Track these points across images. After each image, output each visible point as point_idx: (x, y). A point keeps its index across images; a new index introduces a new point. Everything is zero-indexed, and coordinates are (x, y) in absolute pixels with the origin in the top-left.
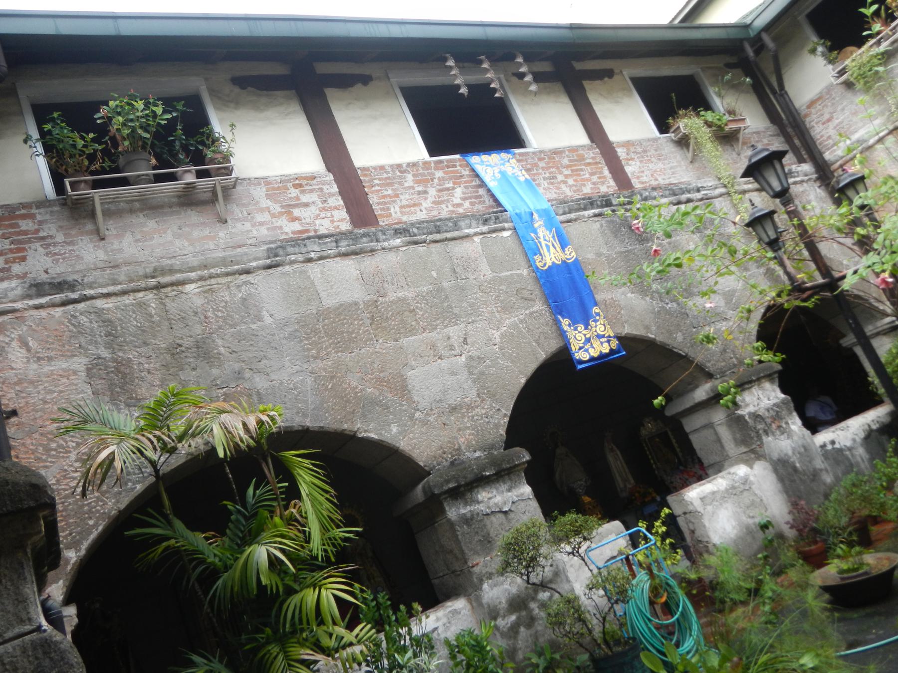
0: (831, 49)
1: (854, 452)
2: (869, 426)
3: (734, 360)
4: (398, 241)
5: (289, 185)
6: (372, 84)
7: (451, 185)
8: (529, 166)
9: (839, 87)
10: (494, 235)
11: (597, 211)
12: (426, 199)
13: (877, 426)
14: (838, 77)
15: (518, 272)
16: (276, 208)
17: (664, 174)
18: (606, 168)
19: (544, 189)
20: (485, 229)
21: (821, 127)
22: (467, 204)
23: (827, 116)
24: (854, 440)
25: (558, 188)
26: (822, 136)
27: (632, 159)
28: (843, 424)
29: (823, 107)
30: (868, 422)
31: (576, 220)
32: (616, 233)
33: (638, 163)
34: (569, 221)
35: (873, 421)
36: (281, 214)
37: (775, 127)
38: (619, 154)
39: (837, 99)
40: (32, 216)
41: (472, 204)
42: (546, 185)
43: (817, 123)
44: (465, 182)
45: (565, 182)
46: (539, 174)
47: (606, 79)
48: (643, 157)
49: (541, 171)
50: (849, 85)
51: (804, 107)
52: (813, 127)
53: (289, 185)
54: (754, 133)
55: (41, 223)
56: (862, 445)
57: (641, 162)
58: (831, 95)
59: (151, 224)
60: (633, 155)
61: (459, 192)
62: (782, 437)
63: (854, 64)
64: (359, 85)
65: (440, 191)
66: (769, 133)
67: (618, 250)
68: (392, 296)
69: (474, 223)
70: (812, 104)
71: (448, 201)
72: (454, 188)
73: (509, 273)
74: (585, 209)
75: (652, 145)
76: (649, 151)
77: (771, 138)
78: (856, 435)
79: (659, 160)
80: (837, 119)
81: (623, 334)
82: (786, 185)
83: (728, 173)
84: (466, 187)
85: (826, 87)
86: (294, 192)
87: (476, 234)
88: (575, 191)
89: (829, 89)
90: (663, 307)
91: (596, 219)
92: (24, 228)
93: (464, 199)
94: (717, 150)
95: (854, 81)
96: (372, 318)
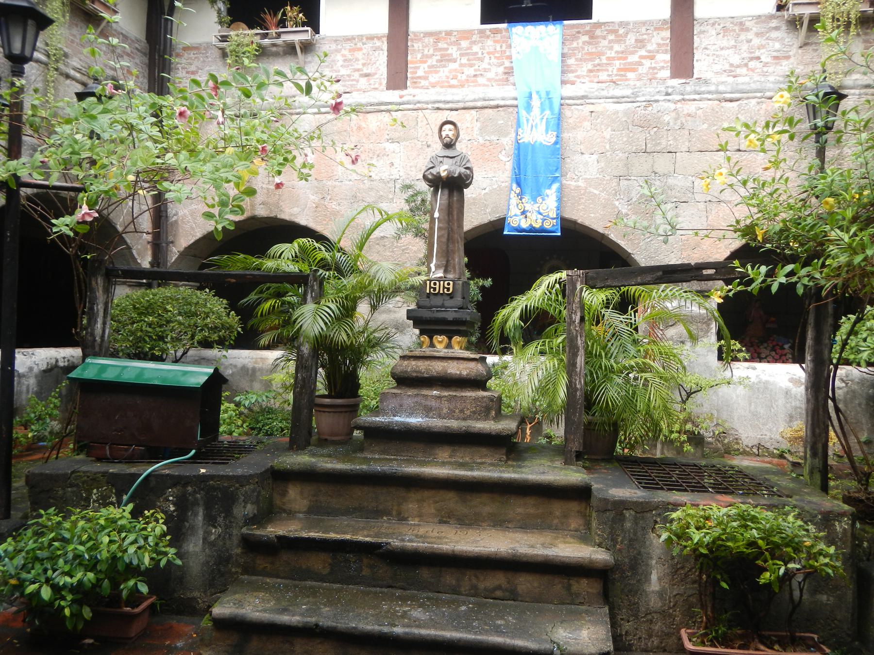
0: (230, 12)
1: (24, 380)
2: (57, 361)
9: (217, 50)
13: (66, 364)
14: (221, 41)
21: (184, 74)
23: (193, 68)
24: (31, 369)
26: (180, 82)
28: (30, 350)
29: (196, 58)
30: (58, 357)
35: (64, 358)
37: (147, 45)
39: (210, 59)
43: (182, 68)
50: (224, 54)
51: (181, 47)
52: (178, 69)
54: (122, 34)
56: (36, 376)
58: (207, 52)
63: (236, 38)
66: (137, 45)
70: (186, 49)
77: (135, 51)
78: (38, 365)
80: (200, 77)
82: (27, 53)
83: (59, 46)
85: (207, 43)
89: (208, 46)
94: (64, 16)
95: (229, 53)
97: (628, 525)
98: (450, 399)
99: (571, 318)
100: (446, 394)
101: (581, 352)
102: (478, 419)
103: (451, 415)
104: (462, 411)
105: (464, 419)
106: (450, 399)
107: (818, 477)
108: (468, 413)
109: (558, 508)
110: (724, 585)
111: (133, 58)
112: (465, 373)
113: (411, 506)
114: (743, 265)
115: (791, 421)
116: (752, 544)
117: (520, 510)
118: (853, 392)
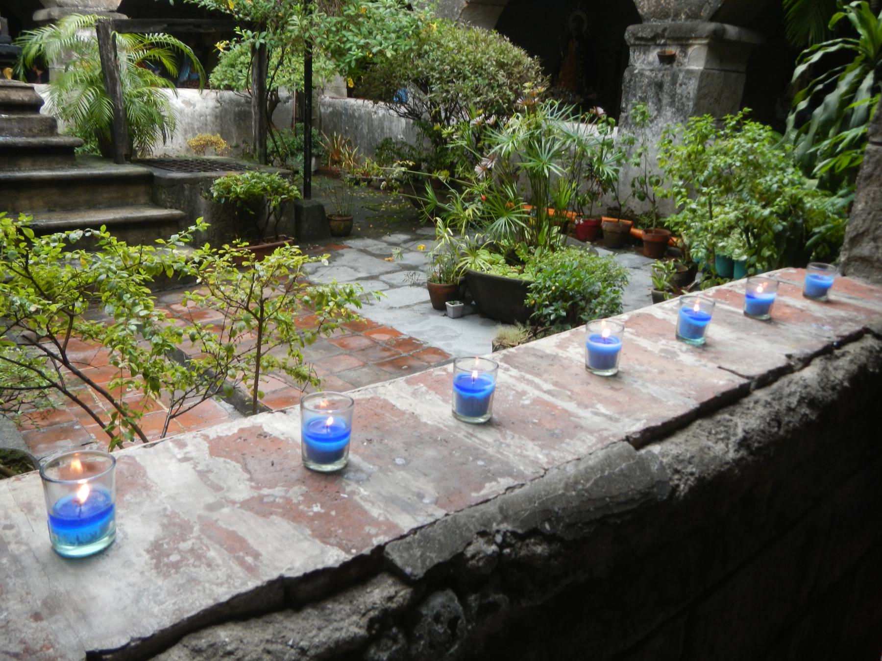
97: (187, 193)
98: (19, 121)
99: (108, 56)
100: (13, 116)
101: (119, 83)
102: (44, 136)
103: (21, 134)
104: (30, 130)
105: (34, 136)
106: (19, 121)
107: (263, 158)
108: (36, 131)
109: (131, 191)
110: (252, 213)
112: (26, 99)
113: (24, 203)
114: (241, 31)
115: (186, 134)
116: (264, 189)
117: (106, 195)
118: (226, 110)
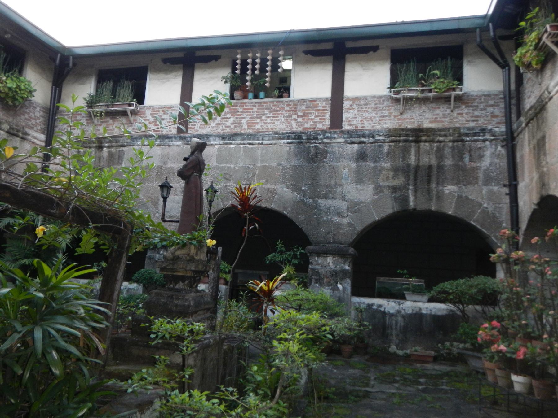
3: (332, 239)
4: (180, 143)
5: (161, 110)
6: (219, 61)
7: (230, 116)
8: (278, 109)
10: (226, 146)
11: (289, 141)
12: (214, 122)
15: (229, 165)
16: (152, 120)
17: (372, 121)
18: (329, 113)
19: (280, 123)
20: (221, 142)
22: (232, 127)
25: (289, 123)
27: (353, 109)
31: (275, 144)
32: (297, 154)
33: (356, 112)
34: (271, 144)
36: (153, 122)
38: (344, 105)
40: (80, 114)
41: (235, 127)
42: (283, 120)
44: (238, 115)
45: (296, 120)
46: (283, 114)
47: (371, 53)
48: (362, 108)
49: (284, 112)
53: (161, 110)
55: (83, 117)
57: (358, 111)
59: (111, 121)
60: (355, 106)
61: (231, 120)
62: (327, 288)
64: (214, 62)
65: (223, 118)
67: (293, 164)
68: (169, 165)
69: (217, 139)
71: (224, 124)
72: (230, 118)
73: (224, 165)
74: (283, 139)
75: (375, 101)
76: (370, 104)
79: (375, 111)
81: (270, 207)
84: (236, 118)
86: (161, 113)
87: (216, 144)
88: (298, 126)
90: (303, 200)
91: (288, 145)
92: (78, 118)
93: (232, 124)
96: (157, 173)
111: (498, 106)
